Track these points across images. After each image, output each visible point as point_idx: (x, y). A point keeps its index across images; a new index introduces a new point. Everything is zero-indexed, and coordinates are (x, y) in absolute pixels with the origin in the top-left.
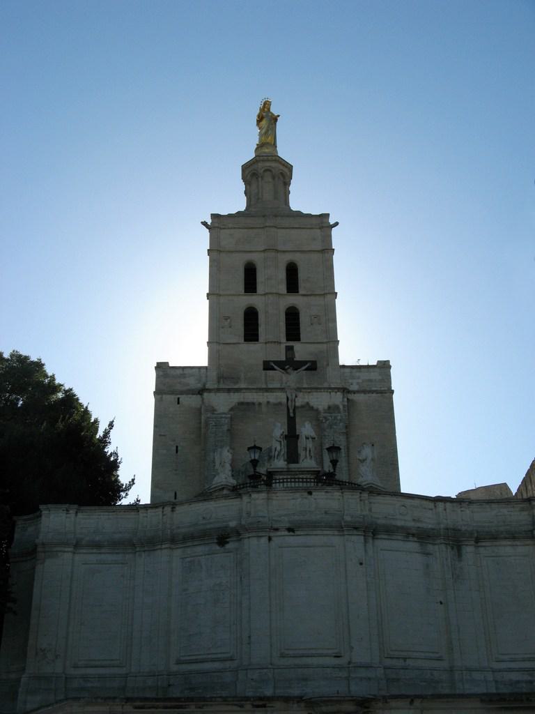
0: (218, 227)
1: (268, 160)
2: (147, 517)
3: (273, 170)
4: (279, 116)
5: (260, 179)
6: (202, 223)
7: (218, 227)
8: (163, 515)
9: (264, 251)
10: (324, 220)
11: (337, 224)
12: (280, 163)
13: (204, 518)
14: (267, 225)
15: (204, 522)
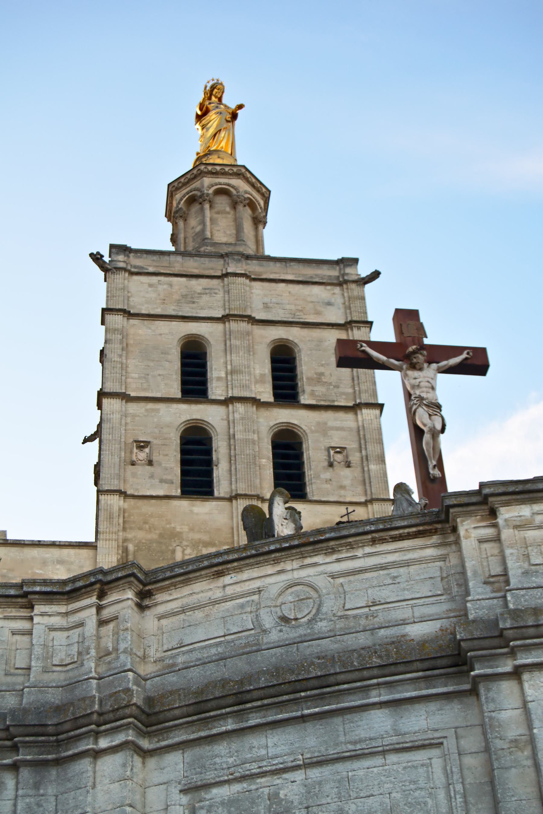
0: (125, 270)
1: (224, 174)
2: (30, 633)
3: (231, 189)
4: (240, 107)
5: (207, 206)
6: (91, 255)
7: (125, 270)
8: (102, 623)
9: (224, 319)
10: (348, 270)
11: (376, 275)
12: (247, 180)
13: (285, 619)
14: (230, 270)
15: (293, 634)
